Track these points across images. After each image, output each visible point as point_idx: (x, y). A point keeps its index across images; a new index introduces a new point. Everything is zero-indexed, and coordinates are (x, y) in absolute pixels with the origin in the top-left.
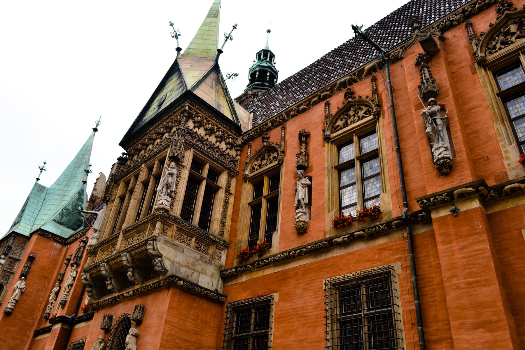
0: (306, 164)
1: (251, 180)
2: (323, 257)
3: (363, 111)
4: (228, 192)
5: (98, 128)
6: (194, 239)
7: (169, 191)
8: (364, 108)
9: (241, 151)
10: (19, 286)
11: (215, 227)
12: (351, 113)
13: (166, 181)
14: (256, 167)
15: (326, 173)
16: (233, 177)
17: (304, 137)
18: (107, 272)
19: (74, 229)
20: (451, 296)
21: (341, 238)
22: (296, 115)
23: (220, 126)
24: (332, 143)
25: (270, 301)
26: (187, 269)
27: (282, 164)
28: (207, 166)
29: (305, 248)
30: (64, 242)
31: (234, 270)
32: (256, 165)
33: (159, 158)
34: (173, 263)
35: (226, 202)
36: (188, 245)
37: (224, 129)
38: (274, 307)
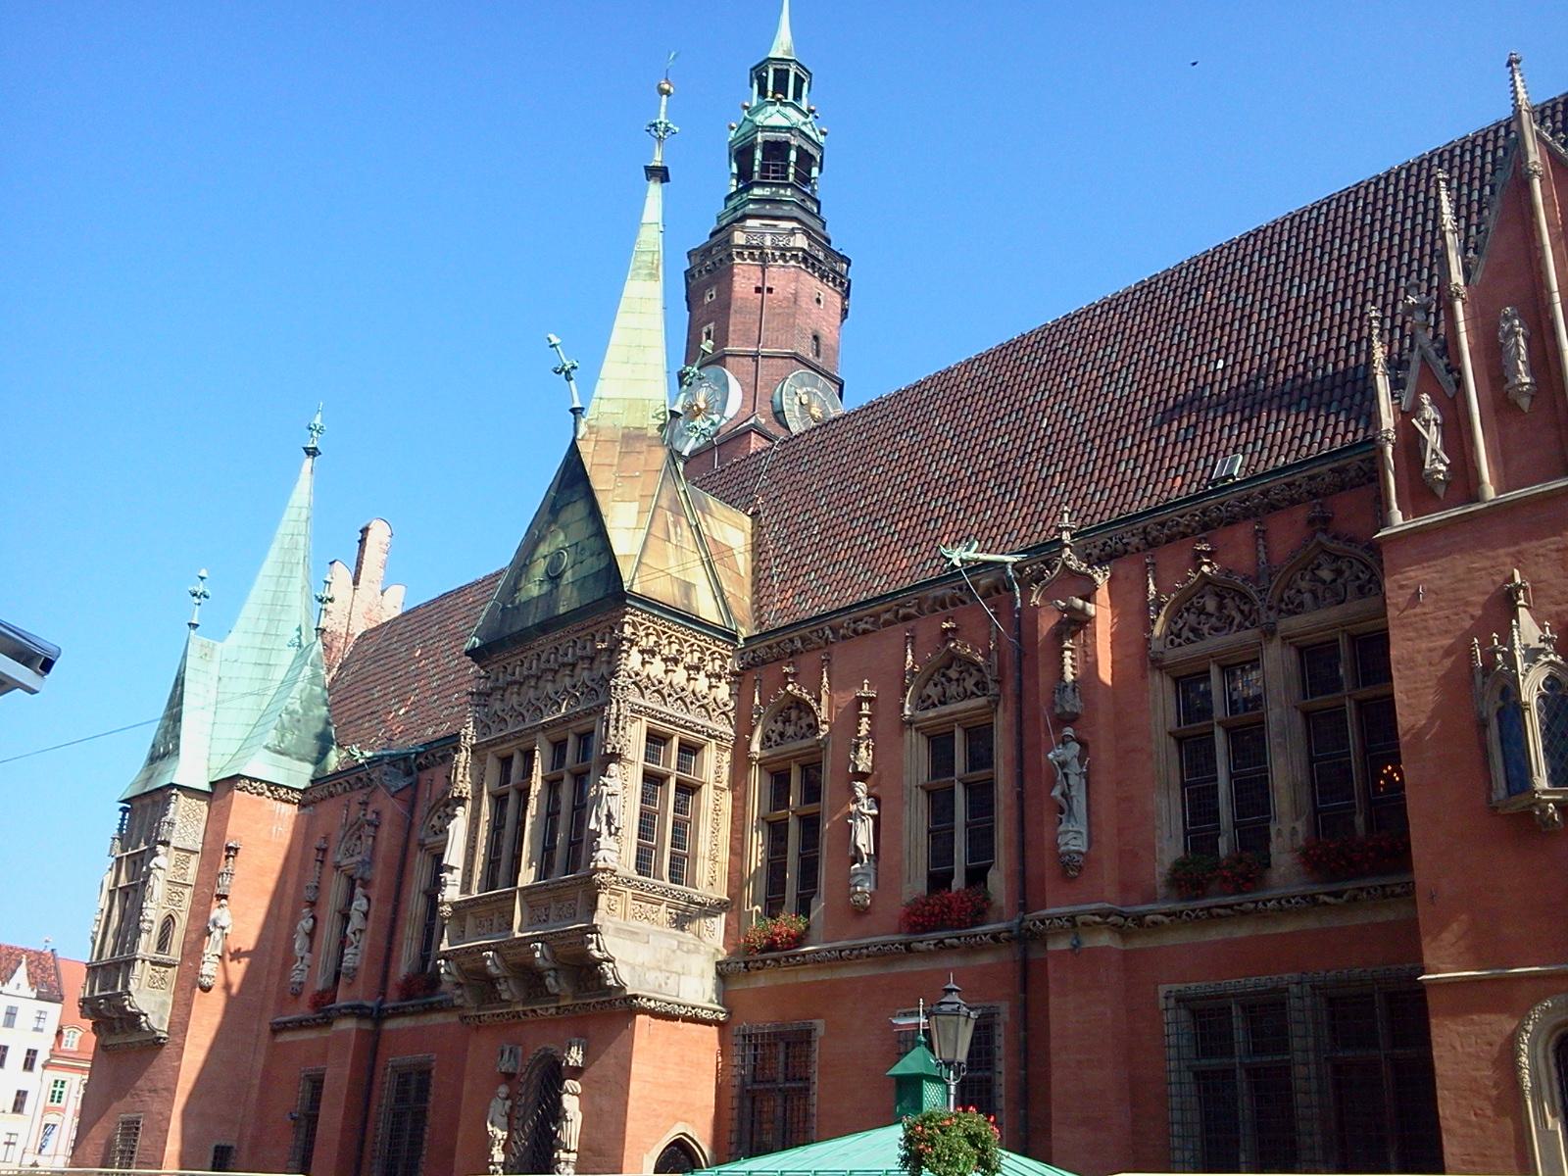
6: (664, 906)
8: (975, 672)
9: (740, 684)
12: (953, 674)
14: (775, 737)
18: (498, 968)
20: (1056, 1075)
24: (917, 729)
25: (809, 1032)
26: (658, 974)
28: (675, 742)
29: (867, 948)
31: (743, 965)
32: (773, 732)
33: (577, 730)
37: (702, 644)
38: (816, 1045)
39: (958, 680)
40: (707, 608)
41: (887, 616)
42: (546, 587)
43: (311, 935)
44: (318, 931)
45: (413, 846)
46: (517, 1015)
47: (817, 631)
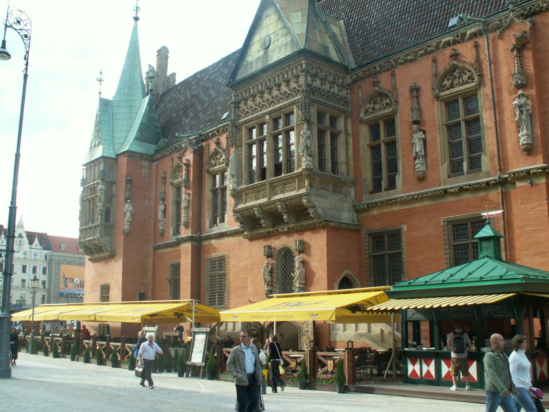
0: (419, 119)
1: (366, 122)
2: (440, 201)
3: (467, 77)
4: (347, 134)
5: (138, 16)
7: (309, 152)
8: (467, 73)
9: (351, 89)
10: (129, 209)
11: (342, 168)
13: (305, 144)
14: (370, 110)
15: (438, 130)
16: (348, 118)
17: (415, 91)
19: (155, 144)
22: (404, 63)
23: (331, 71)
24: (441, 100)
27: (396, 113)
30: (151, 159)
34: (323, 209)
35: (347, 144)
36: (328, 190)
38: (404, 235)
39: (459, 77)
40: (334, 55)
41: (422, 52)
43: (164, 211)
44: (167, 209)
45: (205, 172)
46: (269, 233)
47: (387, 62)
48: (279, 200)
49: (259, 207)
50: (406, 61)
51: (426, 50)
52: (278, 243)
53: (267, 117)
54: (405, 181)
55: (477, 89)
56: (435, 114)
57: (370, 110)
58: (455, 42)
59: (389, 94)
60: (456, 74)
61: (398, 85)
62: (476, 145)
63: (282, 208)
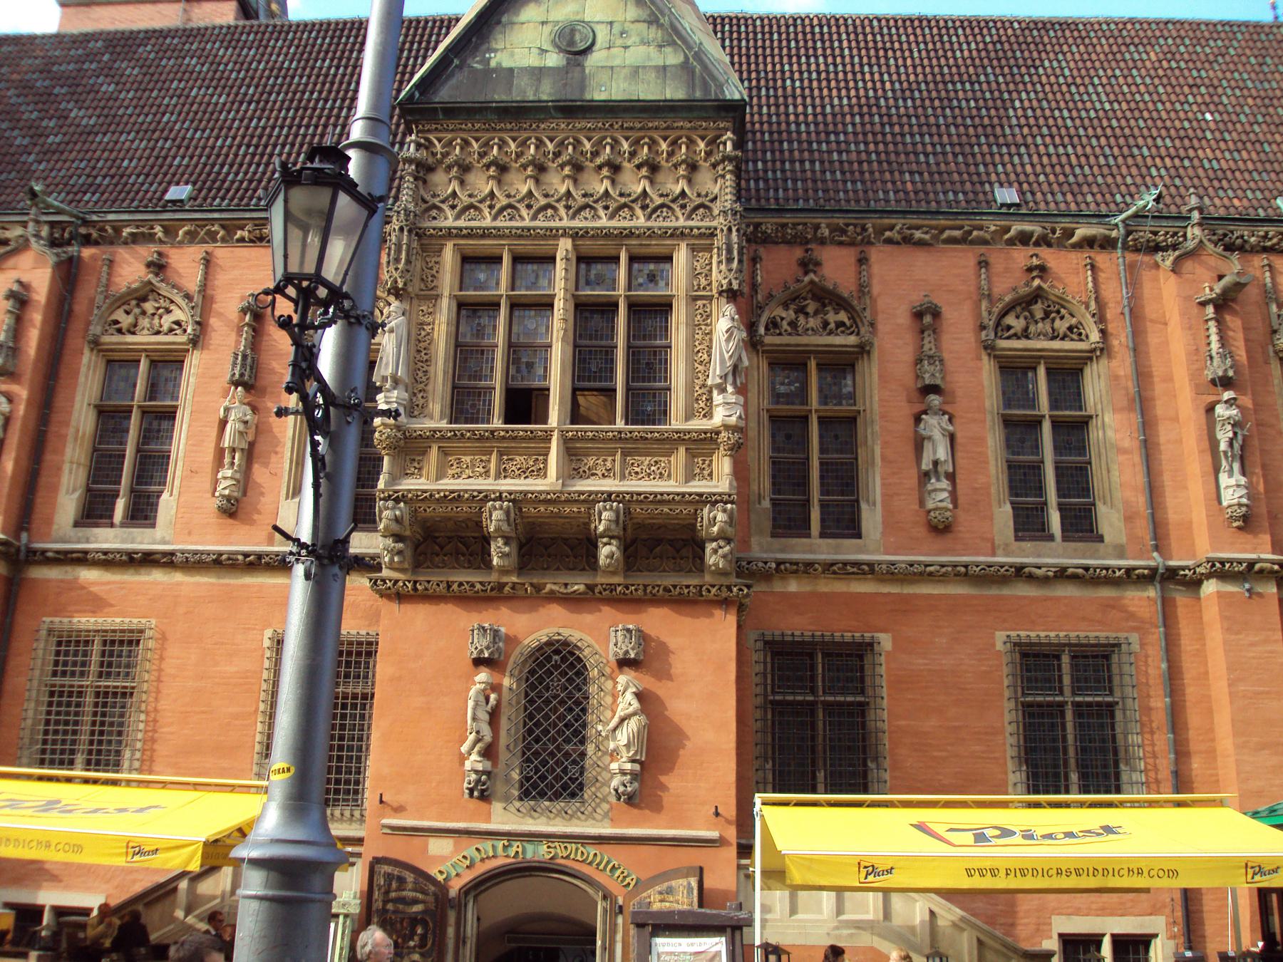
2: (994, 591)
21: (1044, 569)
22: (898, 243)
24: (995, 357)
27: (869, 353)
31: (774, 565)
32: (782, 319)
33: (637, 251)
41: (957, 233)
42: (554, 60)
45: (75, 340)
46: (501, 586)
47: (855, 226)
48: (609, 496)
49: (513, 501)
50: (907, 240)
51: (970, 233)
52: (534, 627)
53: (565, 245)
54: (890, 524)
55: (1091, 359)
56: (979, 384)
57: (785, 323)
58: (1044, 241)
59: (855, 303)
60: (1038, 309)
61: (876, 289)
62: (1076, 480)
63: (617, 521)
